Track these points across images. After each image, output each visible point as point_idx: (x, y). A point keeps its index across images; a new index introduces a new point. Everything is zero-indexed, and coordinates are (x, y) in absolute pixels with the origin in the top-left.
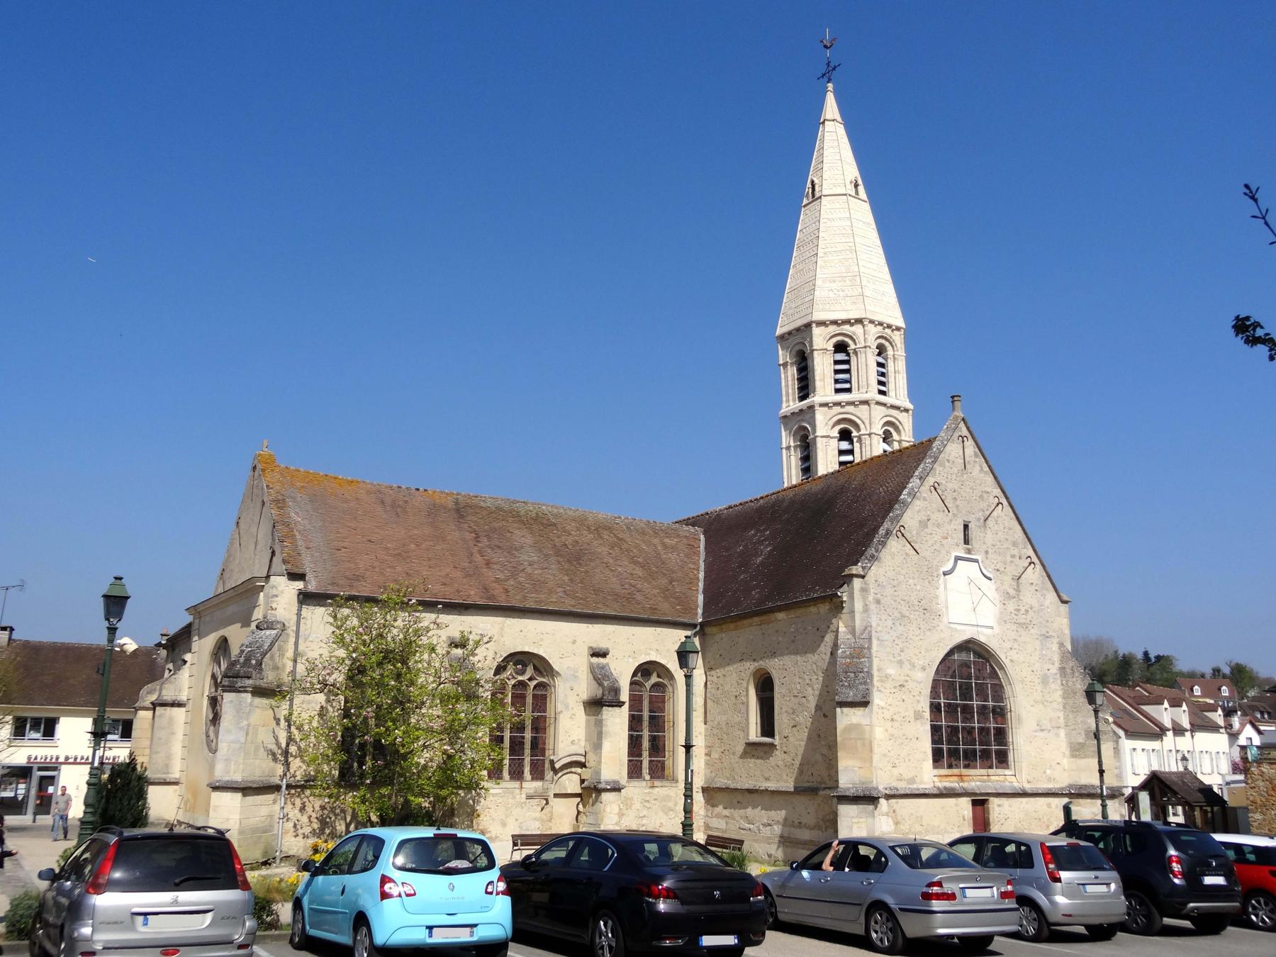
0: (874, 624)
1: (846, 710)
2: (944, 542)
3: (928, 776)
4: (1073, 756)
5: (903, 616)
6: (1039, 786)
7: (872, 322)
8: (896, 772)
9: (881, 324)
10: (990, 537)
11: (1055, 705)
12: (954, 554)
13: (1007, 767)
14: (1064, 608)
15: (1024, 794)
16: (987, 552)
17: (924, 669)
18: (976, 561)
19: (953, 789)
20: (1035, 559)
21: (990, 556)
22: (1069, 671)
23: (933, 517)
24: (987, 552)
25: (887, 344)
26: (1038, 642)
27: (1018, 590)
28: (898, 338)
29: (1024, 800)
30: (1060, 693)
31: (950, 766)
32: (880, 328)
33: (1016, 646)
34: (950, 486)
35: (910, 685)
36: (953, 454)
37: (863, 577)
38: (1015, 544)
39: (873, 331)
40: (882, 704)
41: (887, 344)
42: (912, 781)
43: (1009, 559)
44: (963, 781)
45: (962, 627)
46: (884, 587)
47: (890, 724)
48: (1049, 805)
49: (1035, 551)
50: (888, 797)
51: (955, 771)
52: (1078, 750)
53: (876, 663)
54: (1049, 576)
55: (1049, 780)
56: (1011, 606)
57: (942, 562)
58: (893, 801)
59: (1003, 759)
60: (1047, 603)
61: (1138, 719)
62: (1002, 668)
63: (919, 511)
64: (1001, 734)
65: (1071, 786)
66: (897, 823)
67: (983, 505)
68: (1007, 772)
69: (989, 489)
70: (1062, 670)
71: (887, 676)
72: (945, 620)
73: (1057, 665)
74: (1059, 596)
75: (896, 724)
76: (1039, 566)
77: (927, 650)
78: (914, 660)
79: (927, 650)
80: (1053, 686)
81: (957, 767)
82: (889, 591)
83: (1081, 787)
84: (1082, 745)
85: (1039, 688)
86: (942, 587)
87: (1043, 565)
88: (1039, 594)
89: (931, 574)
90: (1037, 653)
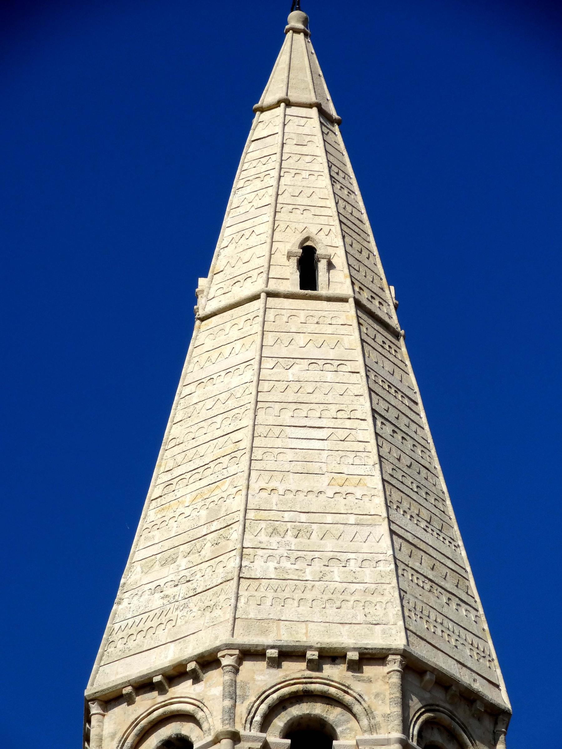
25: (317, 709)
39: (260, 678)
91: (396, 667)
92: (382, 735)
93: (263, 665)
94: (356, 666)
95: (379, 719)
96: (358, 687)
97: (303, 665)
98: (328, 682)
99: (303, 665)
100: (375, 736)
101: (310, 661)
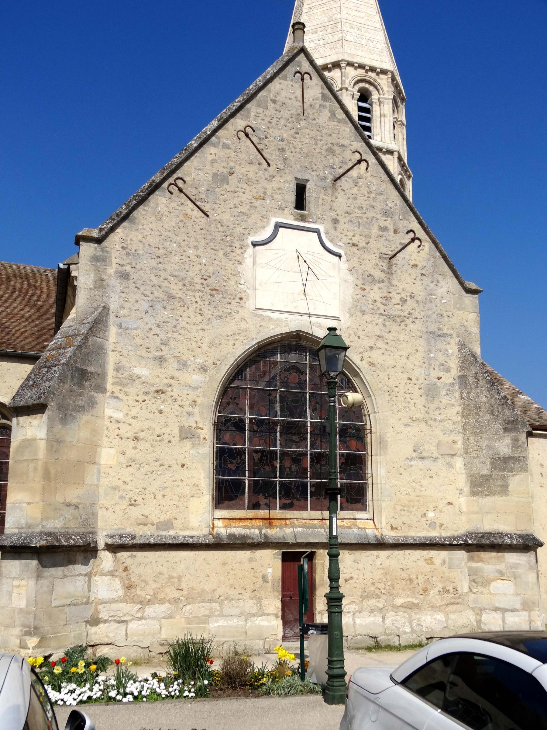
0: (113, 306)
1: (22, 419)
2: (258, 203)
3: (199, 515)
4: (473, 493)
5: (170, 297)
6: (412, 533)
7: (350, 64)
8: (135, 512)
9: (361, 66)
10: (341, 202)
11: (448, 425)
12: (274, 220)
13: (364, 508)
14: (471, 301)
15: (380, 545)
16: (336, 221)
17: (204, 369)
18: (317, 232)
19: (244, 537)
20: (420, 233)
21: (341, 225)
22: (471, 379)
23: (240, 171)
24: (336, 221)
26: (421, 344)
27: (389, 272)
28: (384, 82)
29: (383, 554)
30: (459, 409)
31: (255, 506)
32: (361, 72)
33: (380, 344)
34: (274, 133)
35: (176, 391)
36: (283, 94)
37: (99, 241)
38: (386, 213)
39: (352, 73)
40: (119, 415)
41: (371, 88)
42: (168, 525)
43: (375, 231)
44: (271, 526)
45: (283, 316)
46: (138, 256)
47: (132, 444)
48: (430, 561)
49: (421, 223)
50: (113, 548)
51: (262, 513)
52: (481, 485)
53: (112, 359)
54: (444, 257)
55: (432, 525)
56: (375, 293)
57: (251, 230)
58: (123, 555)
59: (356, 497)
60: (441, 291)
61: (542, 434)
62: (357, 375)
63: (213, 162)
64: (356, 464)
65: (469, 535)
66: (129, 587)
67: (335, 161)
68: (359, 515)
69: (346, 142)
70: (463, 378)
71: (132, 378)
72: (250, 305)
73: (455, 372)
74: (462, 284)
75: (142, 445)
76: (427, 245)
77: (212, 344)
78: (187, 356)
79: (212, 344)
80: (445, 400)
81: (269, 507)
82: (147, 263)
83: (483, 535)
84: (486, 478)
85: (421, 402)
86: (249, 261)
87: (434, 242)
88: (426, 281)
89: (230, 244)
90: (420, 355)
91: (390, 76)
92: (386, 96)
93: (352, 69)
94: (378, 74)
95: (385, 92)
96: (379, 81)
97: (364, 71)
98: (370, 77)
99: (364, 71)
100: (384, 96)
101: (367, 70)
